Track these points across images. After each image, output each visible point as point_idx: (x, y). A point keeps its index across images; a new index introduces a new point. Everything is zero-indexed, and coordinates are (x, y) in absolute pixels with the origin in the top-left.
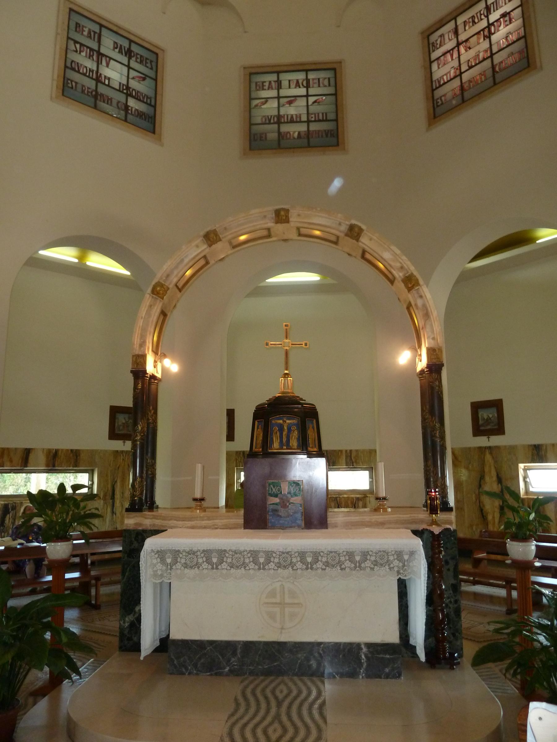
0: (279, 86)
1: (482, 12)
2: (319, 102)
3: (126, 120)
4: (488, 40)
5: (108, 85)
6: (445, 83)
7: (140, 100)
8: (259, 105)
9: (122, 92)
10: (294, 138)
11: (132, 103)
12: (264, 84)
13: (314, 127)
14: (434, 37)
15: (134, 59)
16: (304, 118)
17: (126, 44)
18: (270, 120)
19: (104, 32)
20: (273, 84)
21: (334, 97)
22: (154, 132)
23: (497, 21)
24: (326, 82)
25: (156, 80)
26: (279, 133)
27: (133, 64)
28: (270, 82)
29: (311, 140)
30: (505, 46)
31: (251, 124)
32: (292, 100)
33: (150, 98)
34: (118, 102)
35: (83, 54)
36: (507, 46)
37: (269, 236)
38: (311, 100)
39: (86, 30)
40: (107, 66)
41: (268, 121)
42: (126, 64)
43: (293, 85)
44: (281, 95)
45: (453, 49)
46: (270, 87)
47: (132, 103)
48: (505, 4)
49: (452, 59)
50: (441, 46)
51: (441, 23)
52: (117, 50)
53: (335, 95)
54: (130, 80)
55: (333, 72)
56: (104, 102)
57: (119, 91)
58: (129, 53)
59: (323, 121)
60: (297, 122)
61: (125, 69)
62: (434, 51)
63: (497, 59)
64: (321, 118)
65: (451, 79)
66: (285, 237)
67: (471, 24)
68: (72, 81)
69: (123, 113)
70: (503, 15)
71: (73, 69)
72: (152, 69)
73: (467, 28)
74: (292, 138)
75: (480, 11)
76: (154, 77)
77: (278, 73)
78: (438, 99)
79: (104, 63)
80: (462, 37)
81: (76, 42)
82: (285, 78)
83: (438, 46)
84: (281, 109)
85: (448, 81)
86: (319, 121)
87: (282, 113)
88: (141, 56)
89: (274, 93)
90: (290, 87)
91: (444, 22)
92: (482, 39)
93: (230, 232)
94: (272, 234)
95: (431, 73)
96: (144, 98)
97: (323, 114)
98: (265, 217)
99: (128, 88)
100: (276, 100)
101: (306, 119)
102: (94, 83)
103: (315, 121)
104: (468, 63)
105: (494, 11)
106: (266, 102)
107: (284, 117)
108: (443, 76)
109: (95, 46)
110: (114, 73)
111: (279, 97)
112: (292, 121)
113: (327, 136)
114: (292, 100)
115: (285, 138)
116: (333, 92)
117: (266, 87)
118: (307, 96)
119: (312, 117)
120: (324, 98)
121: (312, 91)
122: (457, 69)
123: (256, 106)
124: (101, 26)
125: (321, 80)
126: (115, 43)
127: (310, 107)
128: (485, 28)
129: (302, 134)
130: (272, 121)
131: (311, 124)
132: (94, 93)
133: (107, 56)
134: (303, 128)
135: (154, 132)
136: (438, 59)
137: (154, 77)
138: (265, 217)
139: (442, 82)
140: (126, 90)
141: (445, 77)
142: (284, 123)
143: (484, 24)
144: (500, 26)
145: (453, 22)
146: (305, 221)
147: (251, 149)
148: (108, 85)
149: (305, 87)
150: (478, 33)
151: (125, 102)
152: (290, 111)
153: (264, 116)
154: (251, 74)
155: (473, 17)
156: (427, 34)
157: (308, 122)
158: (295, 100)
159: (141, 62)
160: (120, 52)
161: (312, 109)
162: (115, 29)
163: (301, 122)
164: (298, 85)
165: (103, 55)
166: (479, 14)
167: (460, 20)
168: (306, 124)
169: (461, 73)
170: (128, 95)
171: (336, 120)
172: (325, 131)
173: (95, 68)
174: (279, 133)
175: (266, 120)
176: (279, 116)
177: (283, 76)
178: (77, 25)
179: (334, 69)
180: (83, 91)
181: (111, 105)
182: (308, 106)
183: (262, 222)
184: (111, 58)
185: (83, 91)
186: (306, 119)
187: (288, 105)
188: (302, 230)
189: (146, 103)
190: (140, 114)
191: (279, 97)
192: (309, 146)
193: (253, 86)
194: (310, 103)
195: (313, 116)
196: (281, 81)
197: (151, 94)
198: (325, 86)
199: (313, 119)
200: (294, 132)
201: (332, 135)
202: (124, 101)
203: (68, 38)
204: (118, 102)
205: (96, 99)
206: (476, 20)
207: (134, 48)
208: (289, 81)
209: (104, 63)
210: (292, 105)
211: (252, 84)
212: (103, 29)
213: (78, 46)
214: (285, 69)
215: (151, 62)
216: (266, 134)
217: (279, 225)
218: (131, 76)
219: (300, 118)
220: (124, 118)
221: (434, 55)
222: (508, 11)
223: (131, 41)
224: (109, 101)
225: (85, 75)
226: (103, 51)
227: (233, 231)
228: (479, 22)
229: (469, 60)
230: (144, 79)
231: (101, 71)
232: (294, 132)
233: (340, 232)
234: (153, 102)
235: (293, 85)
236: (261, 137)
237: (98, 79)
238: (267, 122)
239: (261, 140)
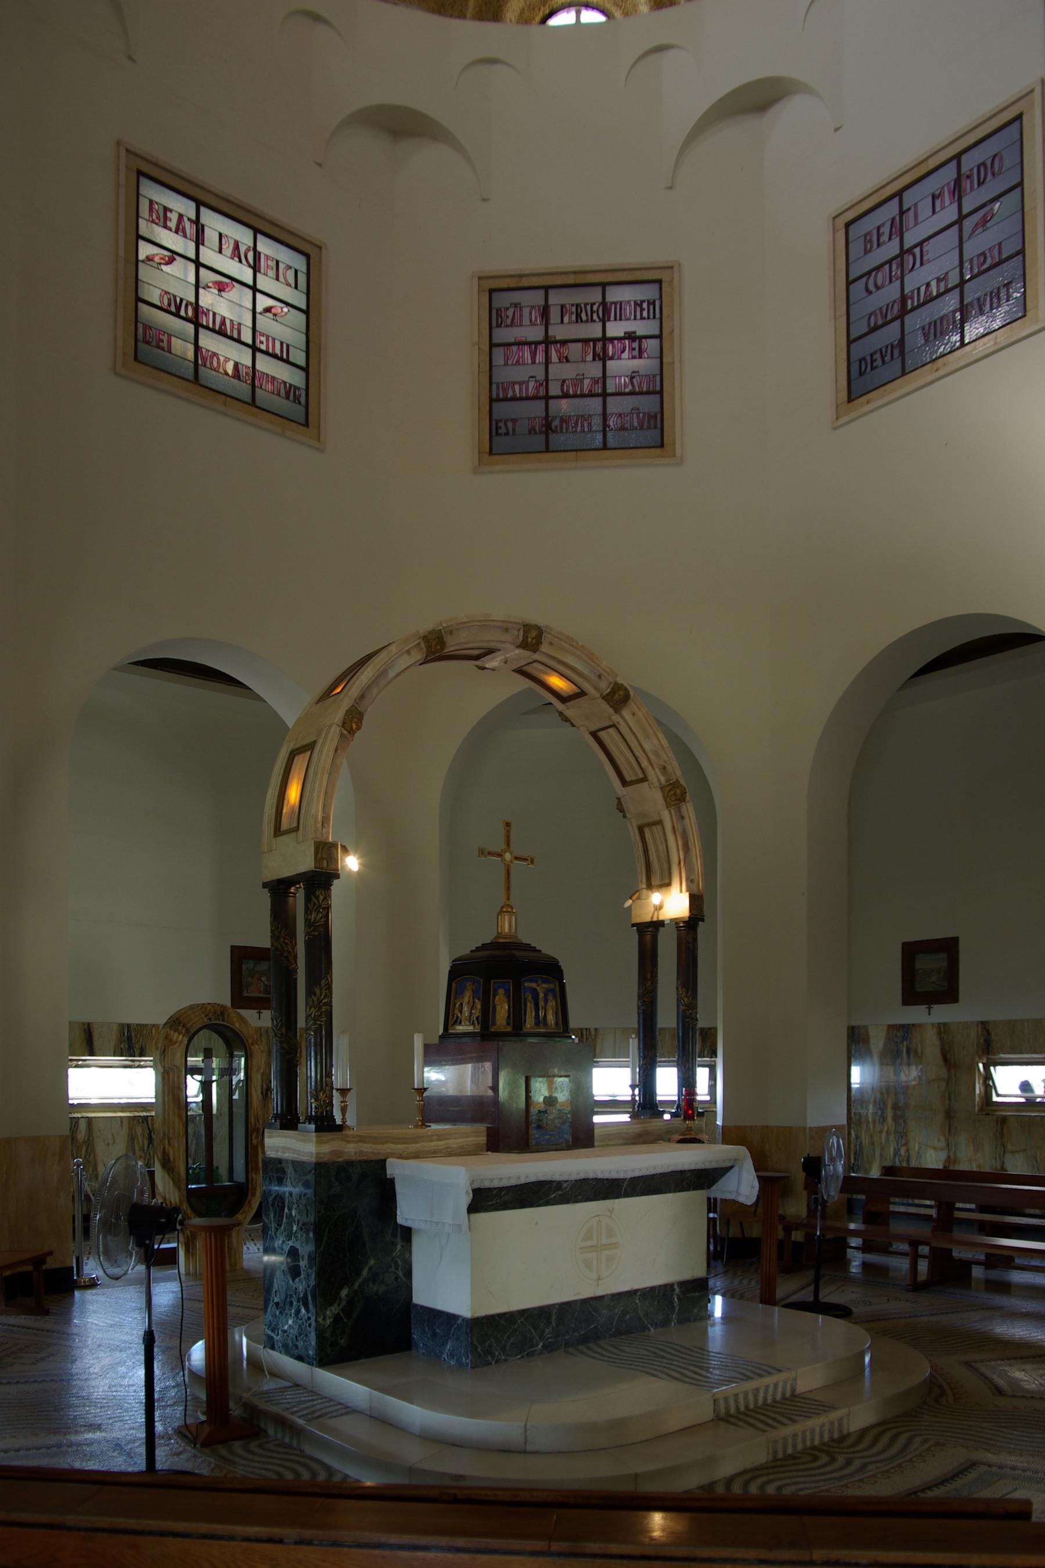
1: (595, 308)
2: (275, 315)
4: (600, 363)
6: (514, 399)
8: (157, 259)
10: (227, 374)
12: (169, 214)
14: (503, 300)
18: (178, 308)
20: (187, 225)
23: (619, 339)
26: (197, 348)
28: (181, 216)
29: (257, 390)
30: (627, 390)
32: (225, 283)
36: (631, 393)
38: (263, 302)
45: (537, 343)
46: (179, 230)
48: (635, 318)
49: (533, 362)
59: (281, 359)
63: (614, 405)
64: (278, 351)
65: (527, 398)
67: (574, 318)
70: (631, 336)
73: (566, 319)
74: (221, 370)
75: (592, 305)
78: (501, 421)
80: (558, 332)
83: (509, 322)
85: (521, 399)
91: (525, 283)
92: (590, 358)
97: (282, 344)
104: (562, 385)
105: (615, 319)
106: (171, 261)
107: (206, 313)
108: (514, 383)
111: (198, 264)
113: (287, 397)
114: (225, 283)
115: (208, 365)
117: (173, 224)
119: (261, 342)
120: (285, 310)
122: (541, 385)
123: (149, 259)
127: (258, 316)
128: (599, 340)
129: (243, 371)
130: (182, 313)
139: (510, 394)
141: (517, 387)
142: (207, 328)
143: (594, 330)
144: (623, 351)
150: (585, 341)
153: (167, 293)
155: (578, 306)
161: (263, 322)
166: (589, 308)
167: (556, 299)
169: (547, 398)
174: (197, 348)
175: (169, 305)
187: (216, 291)
195: (263, 339)
196: (203, 226)
200: (227, 360)
201: (297, 400)
210: (223, 294)
216: (170, 336)
222: (638, 334)
228: (587, 321)
229: (564, 381)
232: (227, 360)
238: (173, 309)
239: (159, 347)
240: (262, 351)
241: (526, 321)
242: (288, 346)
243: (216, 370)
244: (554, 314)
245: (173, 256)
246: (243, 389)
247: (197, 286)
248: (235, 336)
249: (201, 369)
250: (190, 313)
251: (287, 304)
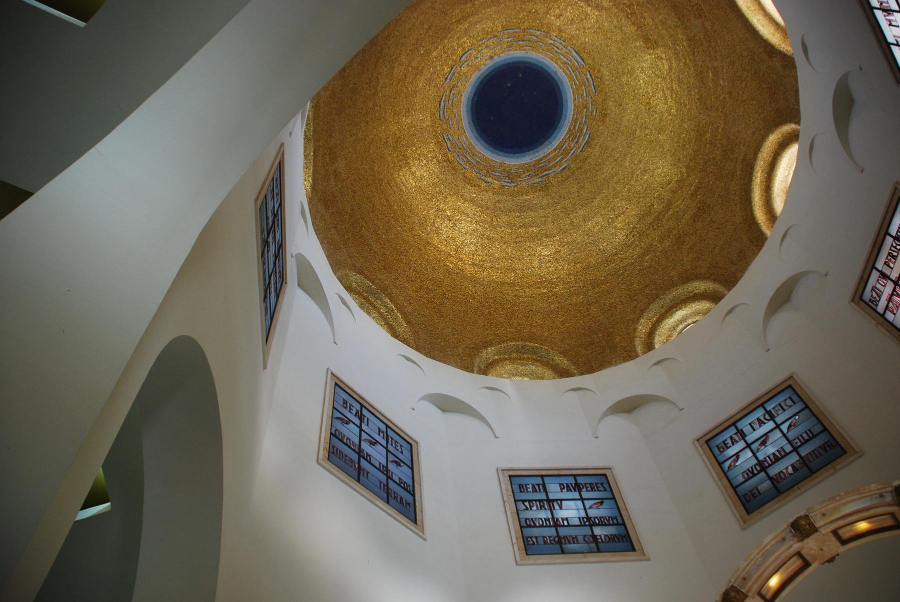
0: (743, 435)
3: (599, 551)
5: (569, 525)
7: (606, 525)
9: (585, 525)
10: (791, 474)
11: (598, 531)
13: (804, 451)
15: (584, 490)
16: (788, 448)
17: (571, 480)
18: (752, 472)
19: (546, 480)
20: (735, 437)
21: (807, 410)
22: (634, 550)
24: (789, 402)
25: (614, 498)
27: (585, 495)
28: (731, 437)
29: (810, 465)
31: (734, 488)
32: (764, 440)
33: (616, 518)
34: (584, 536)
35: (534, 508)
37: (806, 564)
38: (784, 427)
39: (530, 486)
40: (561, 508)
41: (750, 474)
43: (756, 426)
44: (749, 442)
45: (894, 290)
46: (734, 442)
47: (598, 531)
50: (880, 297)
51: (864, 280)
52: (565, 490)
53: (807, 407)
55: (790, 390)
56: (570, 543)
57: (581, 525)
58: (578, 487)
59: (811, 439)
60: (783, 457)
61: (580, 503)
62: (877, 305)
66: (829, 556)
68: (531, 538)
69: (593, 545)
71: (530, 526)
72: (605, 490)
73: (892, 265)
76: (611, 496)
77: (734, 424)
79: (557, 507)
81: (523, 501)
82: (744, 425)
84: (757, 454)
86: (807, 441)
87: (761, 458)
88: (590, 484)
89: (742, 444)
90: (754, 430)
91: (865, 277)
93: (753, 580)
94: (808, 558)
95: (891, 324)
96: (609, 521)
98: (784, 539)
99: (589, 519)
100: (748, 449)
101: (791, 449)
102: (554, 529)
103: (802, 444)
106: (738, 458)
109: (542, 496)
110: (571, 511)
111: (748, 446)
112: (776, 458)
113: (826, 451)
114: (764, 440)
116: (804, 406)
118: (778, 426)
121: (779, 420)
124: (542, 476)
125: (782, 404)
126: (560, 484)
130: (756, 472)
131: (799, 450)
132: (557, 539)
133: (557, 500)
134: (794, 458)
135: (634, 550)
136: (887, 308)
137: (611, 496)
138: (784, 539)
140: (588, 522)
142: (770, 465)
145: (874, 271)
146: (836, 516)
147: (748, 513)
148: (569, 525)
149: (769, 420)
152: (770, 450)
154: (707, 442)
155: (889, 254)
156: (858, 297)
157: (795, 449)
158: (768, 437)
159: (592, 489)
160: (569, 490)
161: (791, 436)
162: (556, 473)
163: (787, 454)
164: (761, 422)
165: (553, 500)
167: (880, 265)
168: (794, 453)
170: (591, 526)
171: (825, 429)
172: (820, 447)
173: (550, 516)
176: (760, 463)
177: (740, 425)
178: (521, 486)
180: (545, 542)
181: (578, 543)
182: (784, 435)
183: (784, 547)
184: (561, 500)
185: (545, 542)
186: (791, 449)
188: (840, 532)
189: (613, 524)
190: (611, 538)
191: (748, 446)
192: (812, 472)
193: (716, 450)
194: (785, 431)
197: (615, 513)
198: (790, 406)
199: (799, 444)
200: (787, 468)
202: (589, 532)
203: (516, 501)
204: (584, 536)
205: (560, 542)
206: (895, 254)
207: (580, 480)
208: (750, 424)
209: (557, 507)
212: (545, 478)
213: (527, 504)
214: (739, 416)
215: (602, 484)
216: (756, 488)
217: (807, 540)
218: (587, 507)
219: (784, 451)
220: (596, 550)
221: (881, 308)
223: (575, 476)
224: (575, 539)
225: (542, 526)
226: (551, 497)
227: (755, 576)
230: (602, 503)
231: (556, 516)
233: (889, 505)
234: (619, 520)
235: (756, 426)
236: (753, 495)
237: (556, 524)
238: (751, 475)
239: (754, 497)
240: (800, 446)
241: (882, 288)
242: (809, 430)
243: (786, 478)
244: (887, 271)
245: (737, 455)
247: (754, 455)
248: (783, 454)
249: (779, 486)
250: (758, 468)
251: (795, 415)
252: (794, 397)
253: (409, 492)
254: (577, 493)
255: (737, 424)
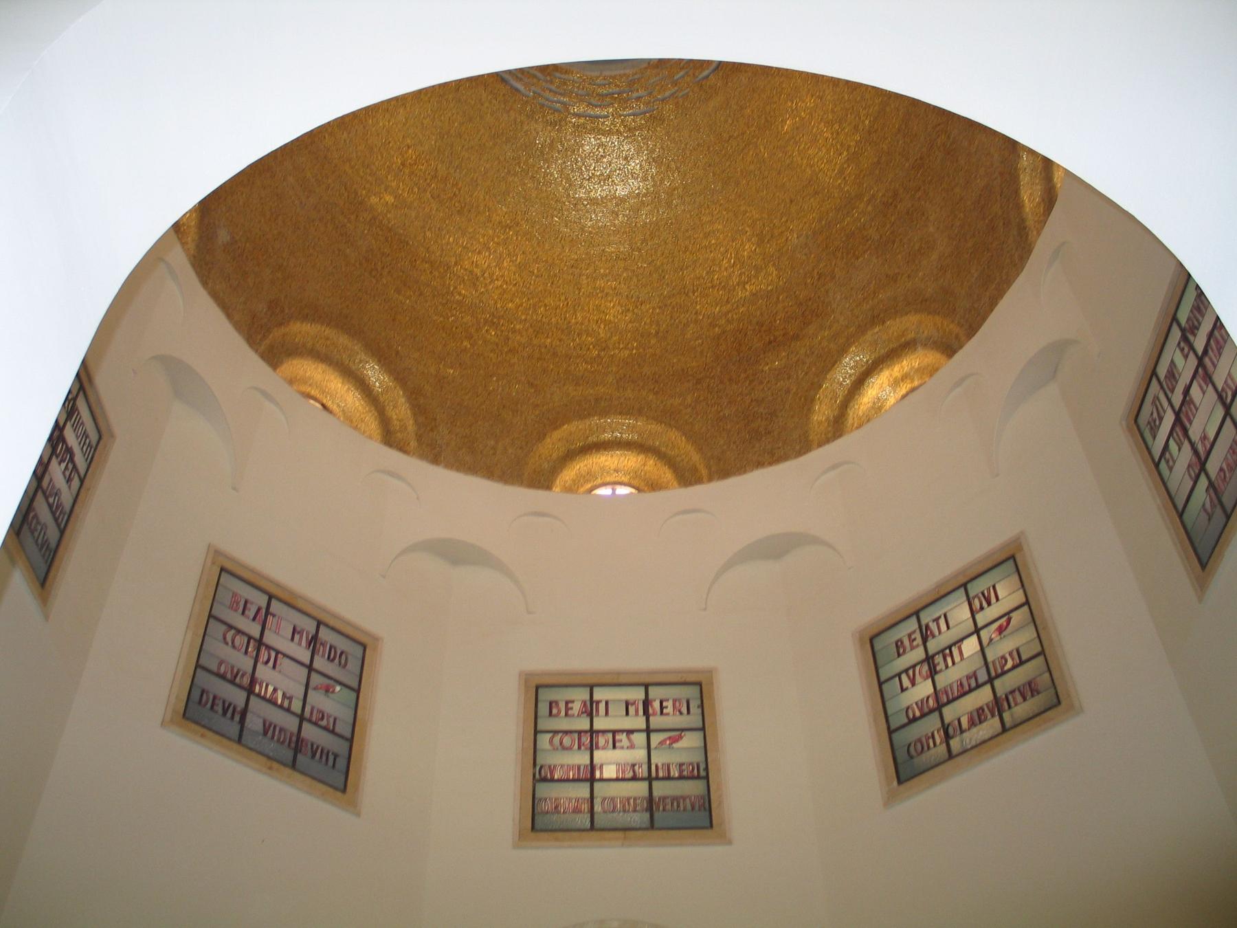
3: (293, 766)
13: (660, 789)
25: (358, 691)
29: (656, 815)
42: (307, 661)
53: (703, 729)
54: (310, 692)
61: (305, 671)
76: (355, 685)
109: (255, 630)
110: (281, 681)
137: (355, 685)
145: (914, 619)
147: (533, 828)
151: (295, 730)
157: (649, 779)
179: (700, 684)
207: (324, 634)
211: (540, 705)
218: (312, 684)
226: (269, 638)
246: (641, 818)
252: (694, 705)
253: (58, 525)
254: (309, 654)
255: (596, 690)
